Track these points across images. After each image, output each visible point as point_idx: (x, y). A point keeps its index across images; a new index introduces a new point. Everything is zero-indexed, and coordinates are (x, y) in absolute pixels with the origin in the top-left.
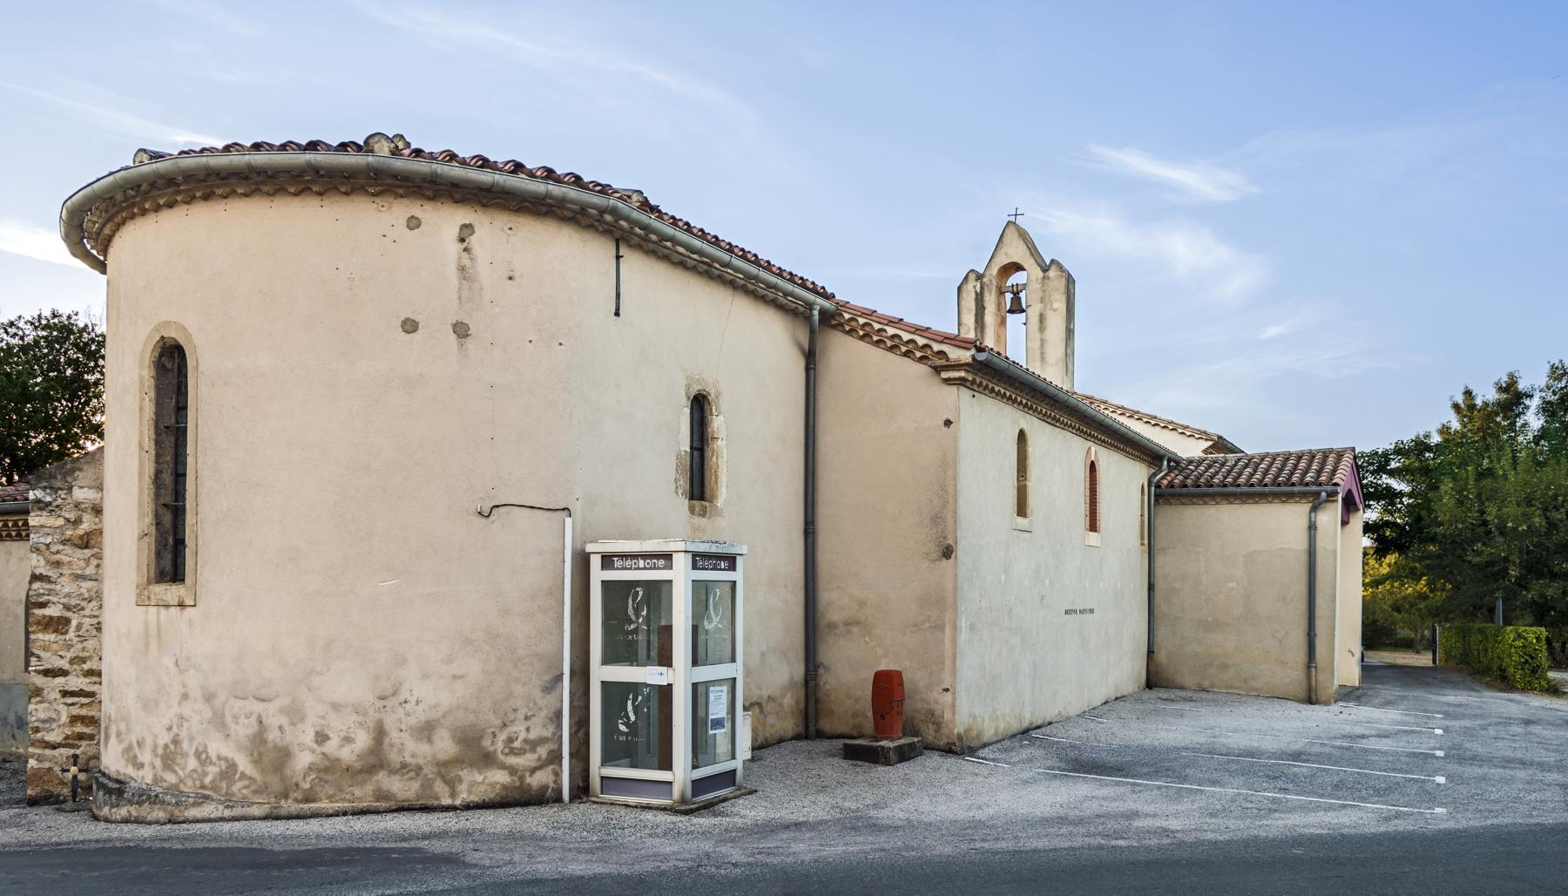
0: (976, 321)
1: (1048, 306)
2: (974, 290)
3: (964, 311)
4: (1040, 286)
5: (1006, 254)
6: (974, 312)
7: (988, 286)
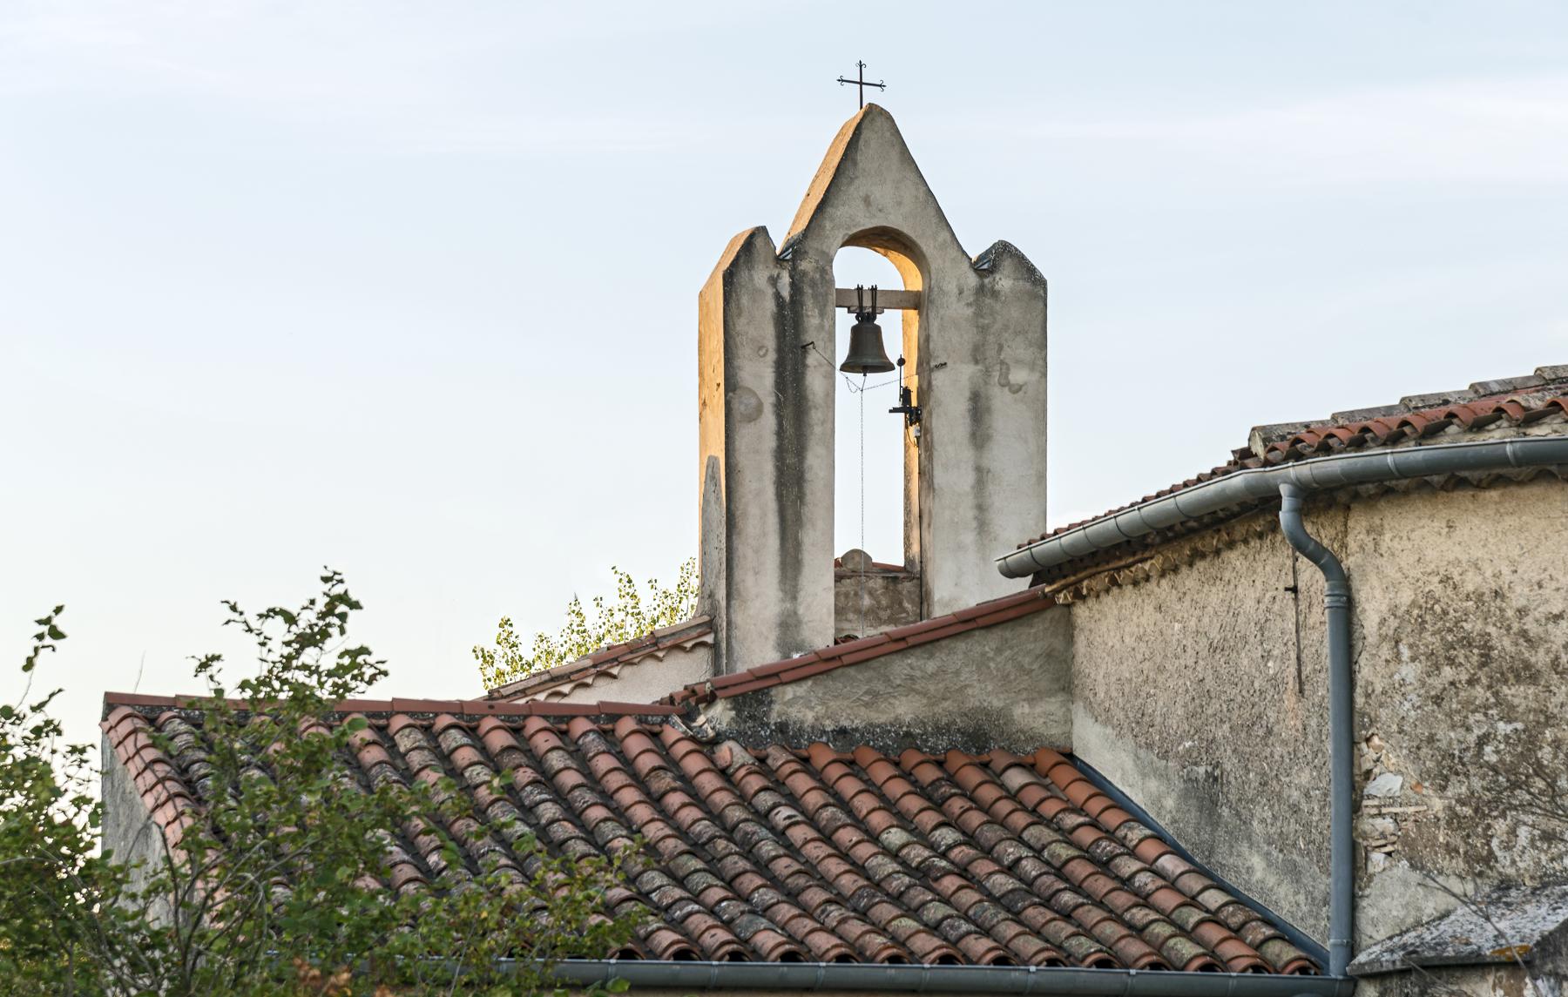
0: (780, 385)
1: (996, 374)
2: (770, 291)
3: (744, 352)
4: (970, 311)
5: (867, 201)
6: (772, 356)
7: (813, 284)
